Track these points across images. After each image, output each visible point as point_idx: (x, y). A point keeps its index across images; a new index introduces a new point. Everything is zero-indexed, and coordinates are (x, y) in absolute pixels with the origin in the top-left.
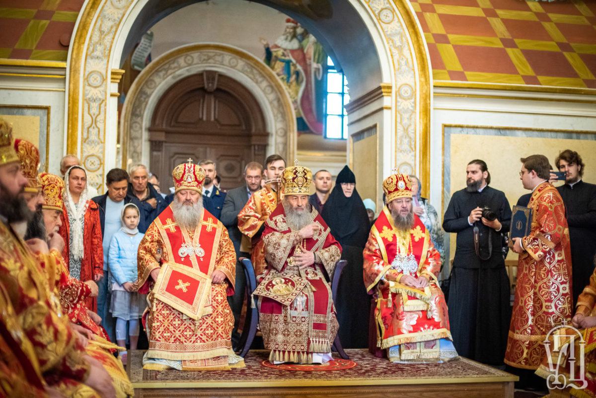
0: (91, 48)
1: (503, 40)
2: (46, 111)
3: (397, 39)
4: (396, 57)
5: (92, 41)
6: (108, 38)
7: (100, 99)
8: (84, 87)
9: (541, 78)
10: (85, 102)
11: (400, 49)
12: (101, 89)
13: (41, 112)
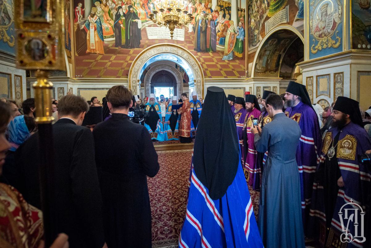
1: (220, 69)
3: (197, 70)
4: (197, 74)
6: (136, 73)
9: (228, 77)
11: (197, 72)
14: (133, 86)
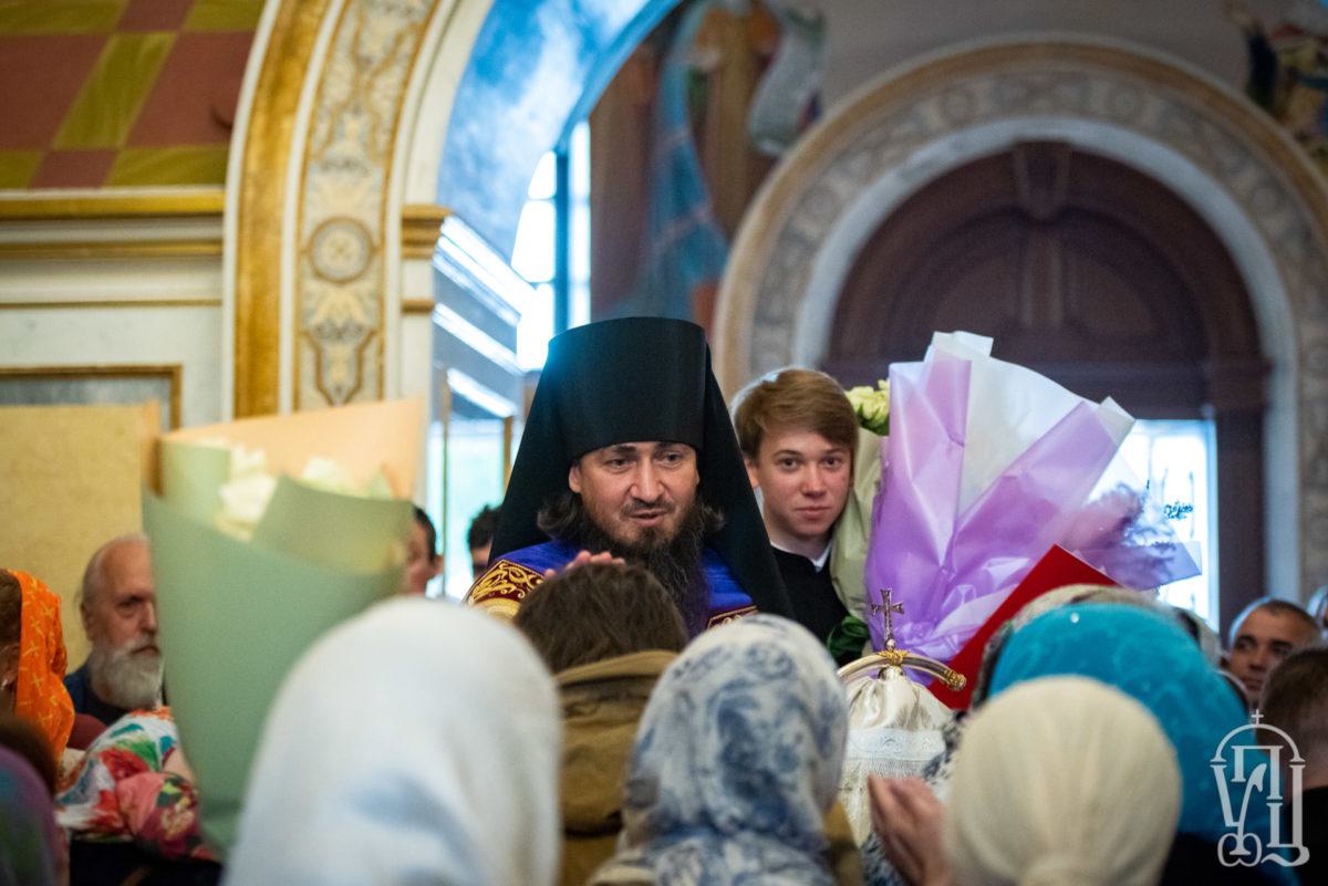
0: (322, 129)
2: (165, 385)
5: (328, 102)
6: (388, 82)
7: (360, 328)
8: (298, 286)
10: (304, 342)
12: (366, 286)
13: (146, 388)
14: (315, 338)
